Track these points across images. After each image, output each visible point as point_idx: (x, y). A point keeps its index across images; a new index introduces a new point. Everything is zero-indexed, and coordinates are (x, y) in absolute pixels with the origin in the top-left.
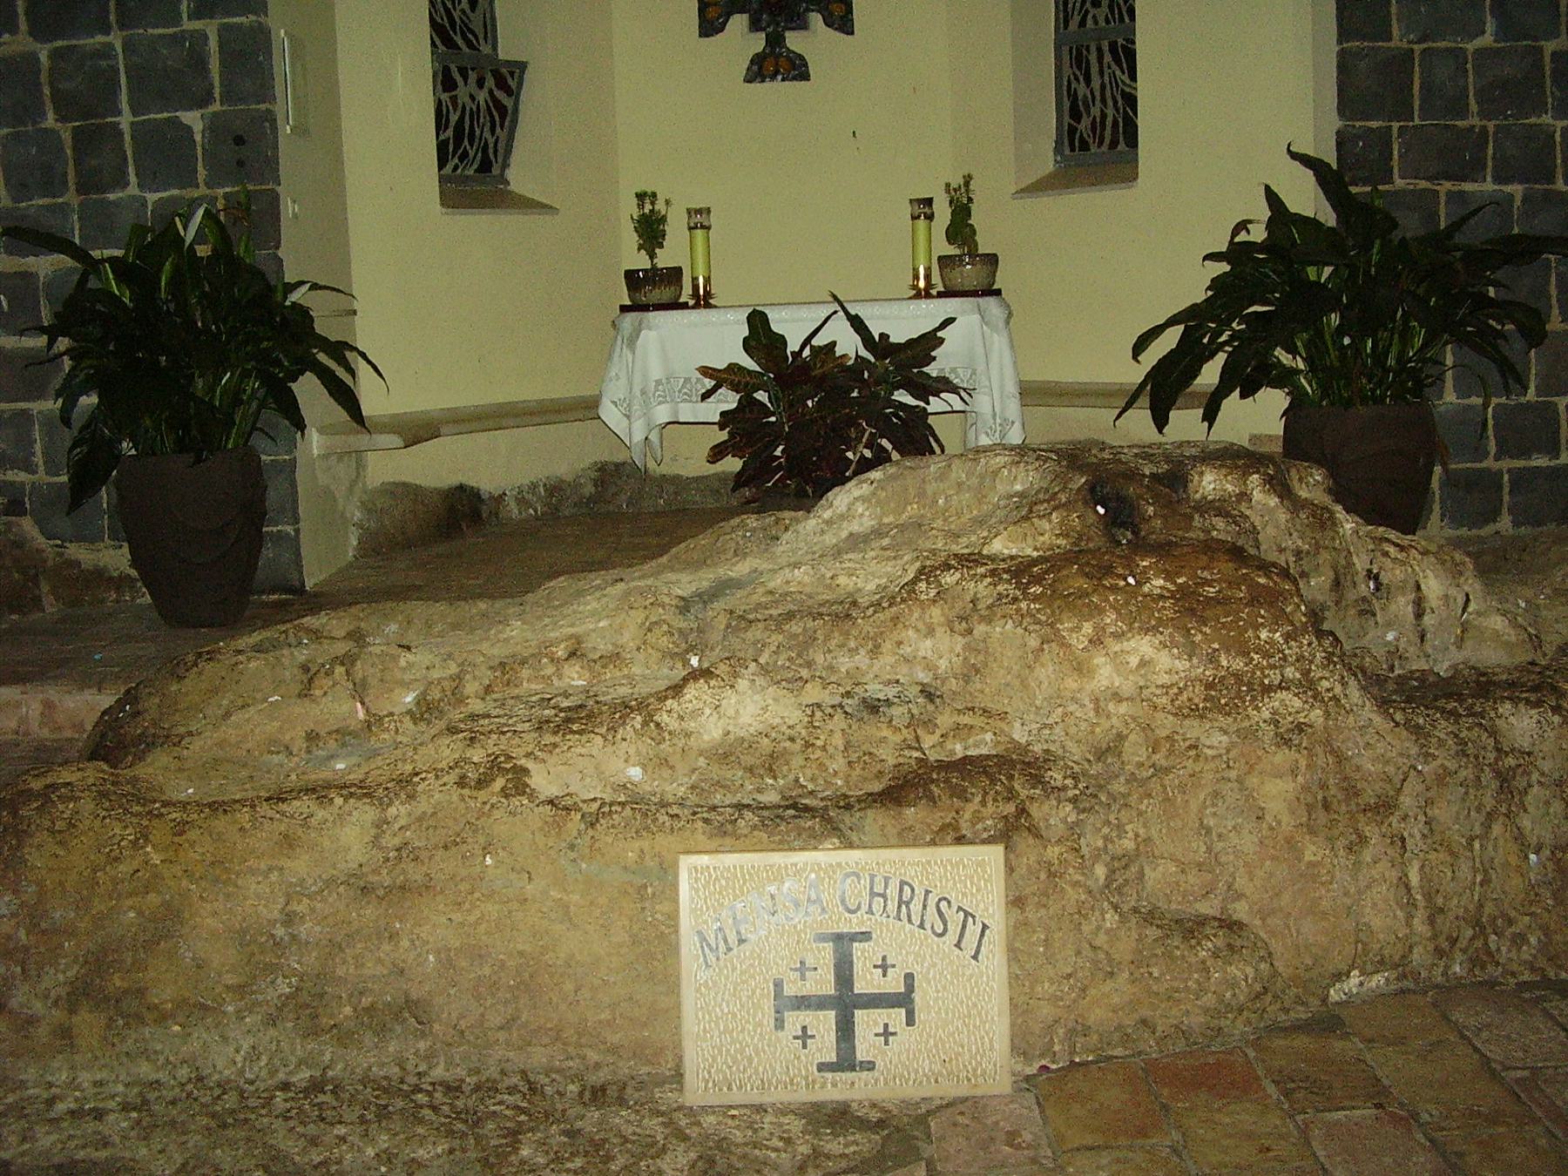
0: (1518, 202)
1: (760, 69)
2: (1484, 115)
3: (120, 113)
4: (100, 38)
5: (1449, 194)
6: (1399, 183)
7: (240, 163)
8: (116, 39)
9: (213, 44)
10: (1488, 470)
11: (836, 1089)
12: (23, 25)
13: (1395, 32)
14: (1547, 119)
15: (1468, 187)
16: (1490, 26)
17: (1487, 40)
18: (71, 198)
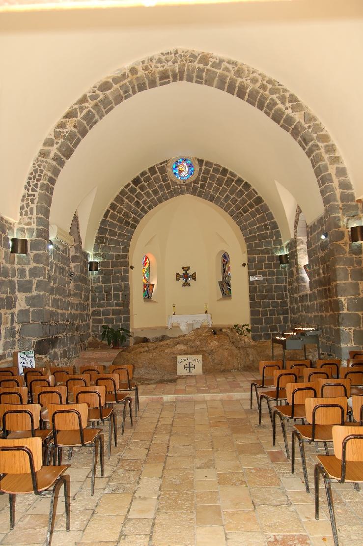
1: (184, 285)
6: (256, 301)
8: (112, 284)
9: (123, 285)
11: (189, 374)
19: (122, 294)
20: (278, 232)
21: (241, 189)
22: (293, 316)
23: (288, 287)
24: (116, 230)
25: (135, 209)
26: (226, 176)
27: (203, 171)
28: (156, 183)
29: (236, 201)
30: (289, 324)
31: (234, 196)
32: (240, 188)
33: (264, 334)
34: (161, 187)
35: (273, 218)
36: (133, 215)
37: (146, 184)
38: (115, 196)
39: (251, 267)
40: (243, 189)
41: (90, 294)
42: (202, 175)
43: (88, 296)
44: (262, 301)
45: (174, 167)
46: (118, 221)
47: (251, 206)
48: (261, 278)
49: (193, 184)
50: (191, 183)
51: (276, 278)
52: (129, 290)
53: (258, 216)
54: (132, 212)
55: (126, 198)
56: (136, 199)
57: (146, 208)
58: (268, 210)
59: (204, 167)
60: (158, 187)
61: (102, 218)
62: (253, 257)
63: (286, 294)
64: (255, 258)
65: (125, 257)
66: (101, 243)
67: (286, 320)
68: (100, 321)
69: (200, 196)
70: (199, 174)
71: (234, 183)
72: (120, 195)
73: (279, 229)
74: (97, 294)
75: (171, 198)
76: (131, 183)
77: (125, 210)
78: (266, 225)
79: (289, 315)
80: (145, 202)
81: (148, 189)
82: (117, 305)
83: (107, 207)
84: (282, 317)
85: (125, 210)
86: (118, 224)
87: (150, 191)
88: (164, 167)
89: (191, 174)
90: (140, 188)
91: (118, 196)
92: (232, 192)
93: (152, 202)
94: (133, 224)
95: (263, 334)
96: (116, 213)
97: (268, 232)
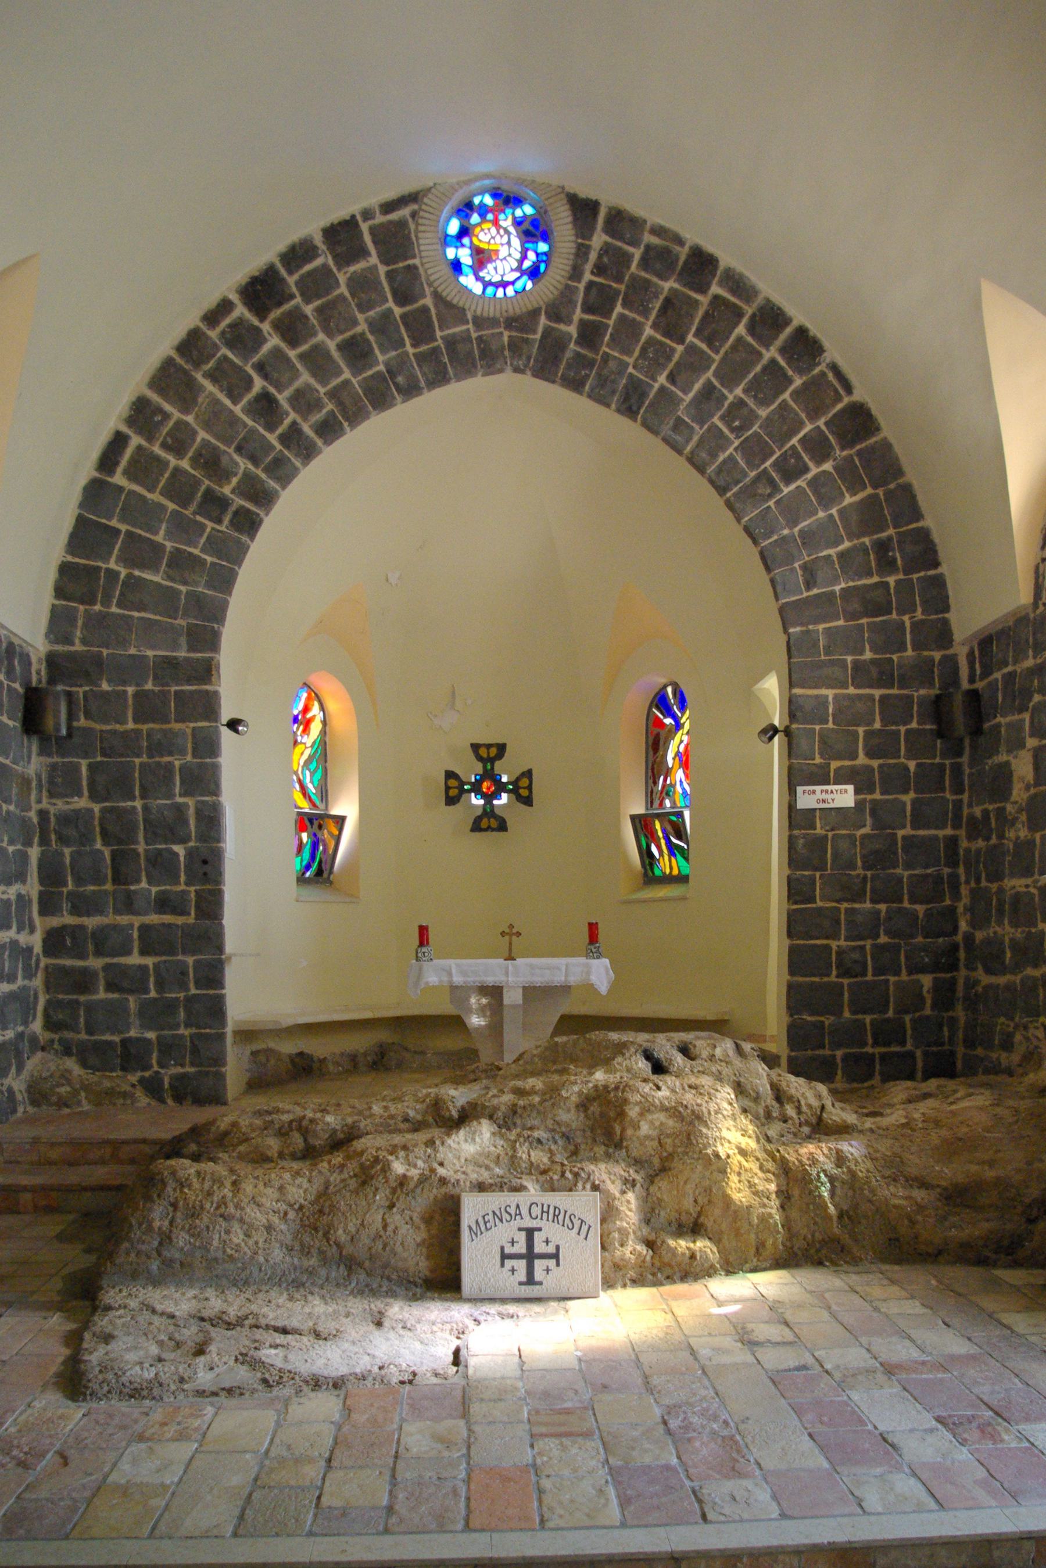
0: (883, 914)
2: (865, 868)
3: (138, 843)
4: (129, 803)
5: (846, 910)
6: (820, 904)
7: (205, 874)
8: (138, 804)
9: (191, 811)
10: (867, 1053)
12: (86, 793)
13: (818, 825)
14: (898, 871)
15: (856, 906)
16: (869, 821)
17: (866, 830)
18: (109, 887)
19: (190, 854)
20: (939, 582)
21: (773, 361)
22: (986, 980)
23: (964, 844)
24: (159, 538)
25: (253, 431)
26: (703, 289)
27: (593, 256)
28: (363, 307)
29: (753, 417)
30: (960, 1013)
31: (739, 391)
32: (772, 353)
33: (845, 1058)
34: (383, 326)
35: (918, 516)
36: (243, 464)
37: (309, 310)
38: (153, 361)
39: (803, 744)
40: (782, 363)
41: (34, 853)
42: (588, 276)
43: (24, 857)
44: (845, 905)
45: (454, 227)
46: (167, 493)
47: (818, 447)
48: (844, 796)
49: (543, 321)
50: (535, 313)
51: (914, 802)
52: (219, 839)
53: (848, 500)
54: (239, 449)
55: (212, 376)
56: (259, 384)
57: (307, 429)
58: (899, 472)
59: (599, 239)
60: (371, 324)
61: (87, 471)
62: (817, 697)
63: (954, 877)
64: (823, 701)
65: (207, 671)
66: (82, 602)
67: (945, 996)
68: (83, 982)
69: (575, 385)
70: (576, 273)
71: (741, 330)
72: (179, 360)
73: (943, 569)
74: (67, 851)
75: (432, 384)
76: (234, 297)
77: (202, 435)
78: (883, 547)
79: (963, 972)
80: (303, 401)
81: (321, 337)
82: (164, 904)
83: (113, 421)
84: (927, 981)
85: (202, 435)
86: (171, 506)
87: (332, 345)
88: (402, 224)
89: (534, 273)
90: (277, 326)
91: (168, 363)
92: (730, 375)
93: (340, 404)
94: (240, 512)
95: (839, 1053)
96: (157, 450)
97: (891, 580)
